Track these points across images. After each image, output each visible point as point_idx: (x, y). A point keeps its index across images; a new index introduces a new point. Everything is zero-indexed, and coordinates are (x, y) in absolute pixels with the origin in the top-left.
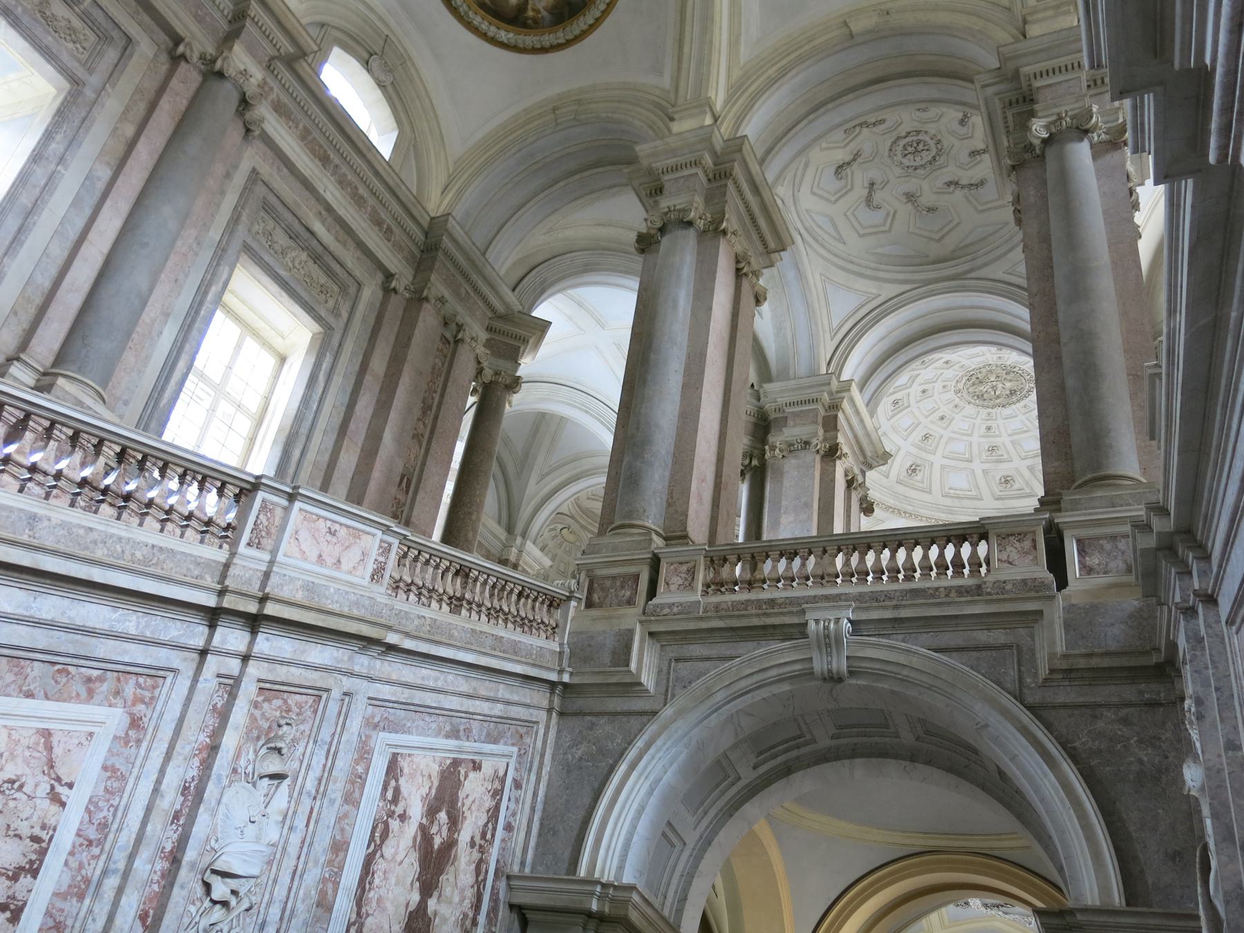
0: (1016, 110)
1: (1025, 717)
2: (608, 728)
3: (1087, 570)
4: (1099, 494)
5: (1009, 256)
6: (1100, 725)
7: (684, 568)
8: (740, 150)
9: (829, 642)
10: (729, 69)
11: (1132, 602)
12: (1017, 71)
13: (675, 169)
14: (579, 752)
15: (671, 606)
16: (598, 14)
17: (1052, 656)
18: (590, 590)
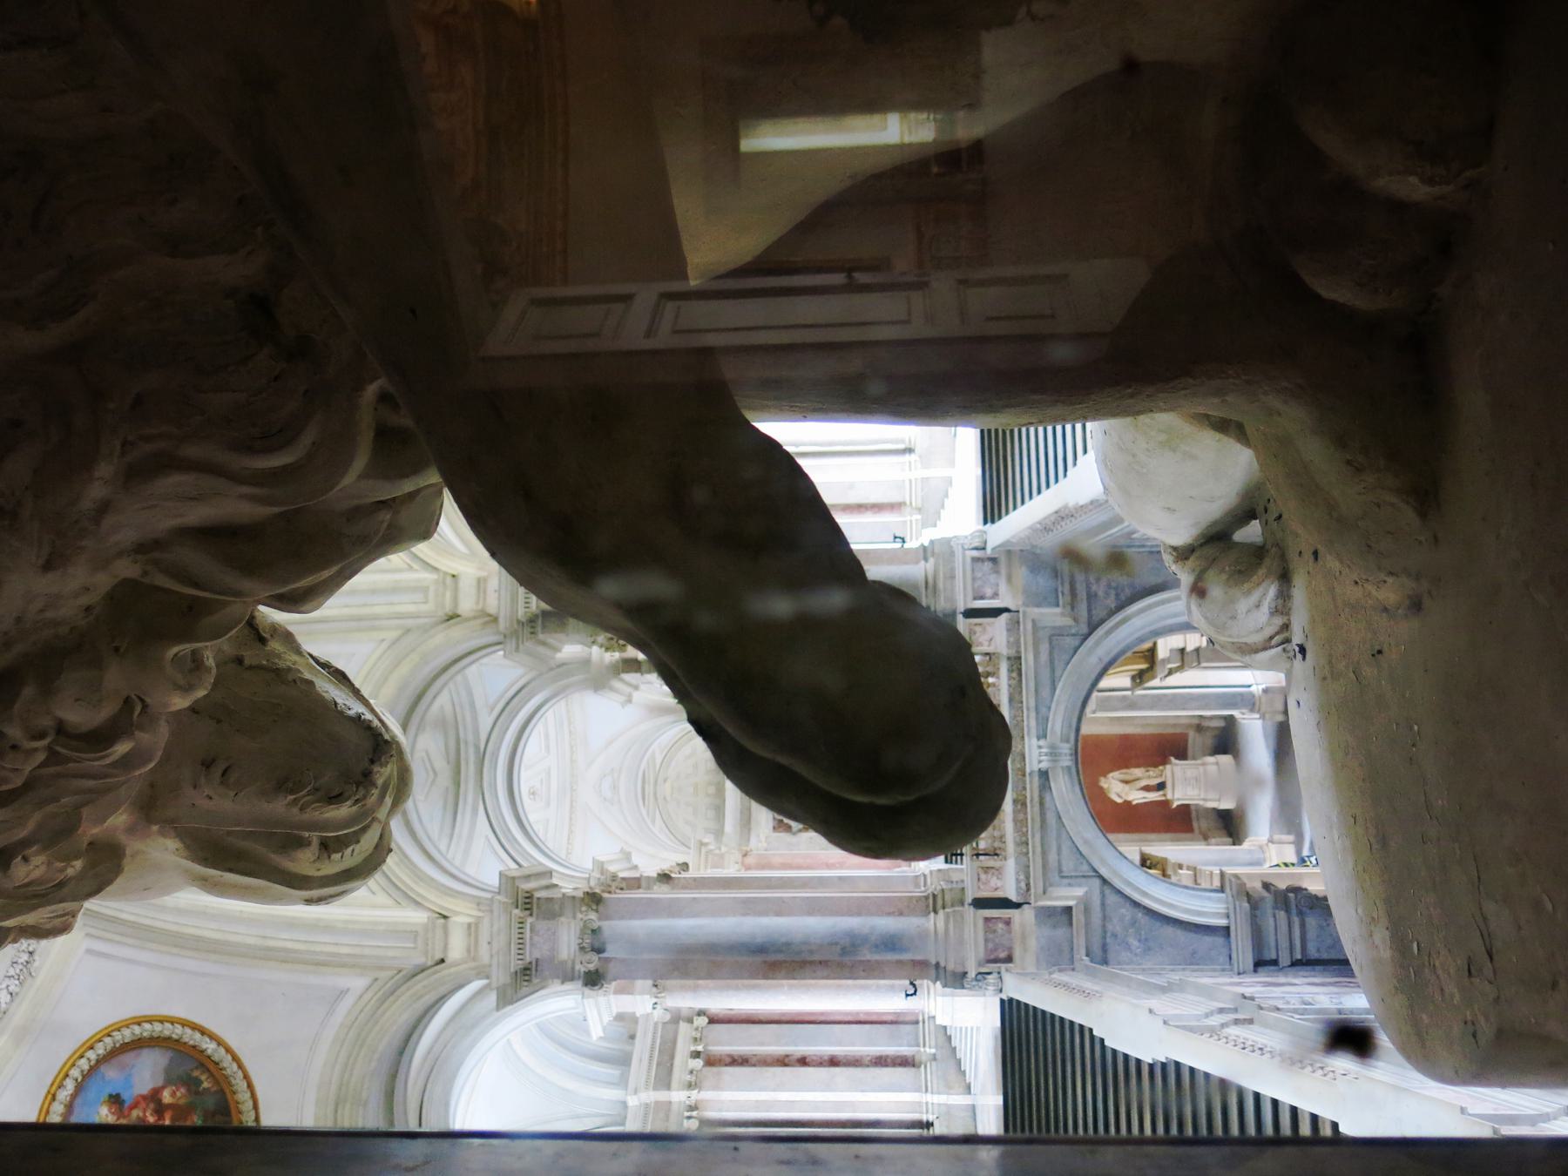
0: (539, 629)
1: (1100, 632)
2: (1115, 921)
3: (995, 595)
4: (941, 585)
5: (479, 703)
6: (1101, 593)
7: (983, 877)
8: (513, 878)
9: (1054, 754)
10: (374, 906)
11: (1021, 573)
12: (518, 622)
13: (521, 944)
14: (1136, 943)
15: (1018, 881)
16: (240, 1074)
17: (1063, 614)
18: (996, 961)
